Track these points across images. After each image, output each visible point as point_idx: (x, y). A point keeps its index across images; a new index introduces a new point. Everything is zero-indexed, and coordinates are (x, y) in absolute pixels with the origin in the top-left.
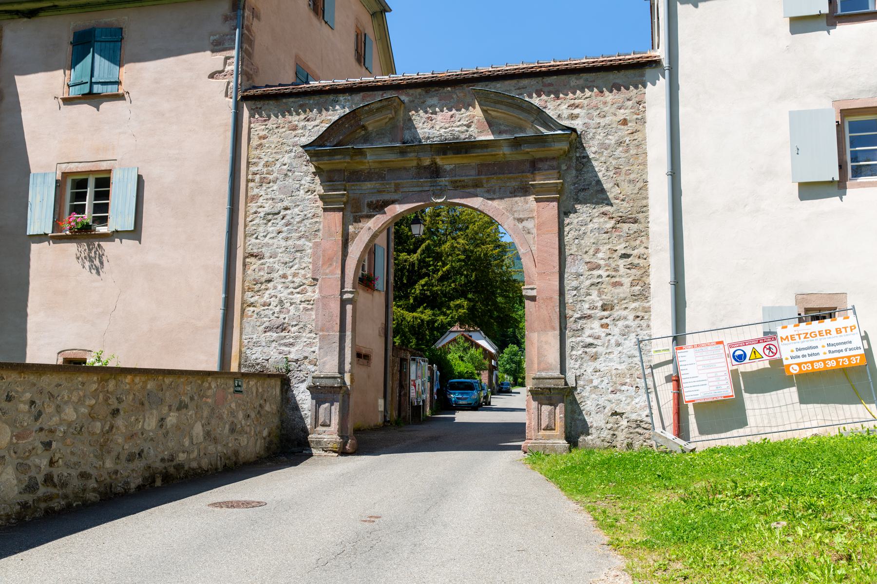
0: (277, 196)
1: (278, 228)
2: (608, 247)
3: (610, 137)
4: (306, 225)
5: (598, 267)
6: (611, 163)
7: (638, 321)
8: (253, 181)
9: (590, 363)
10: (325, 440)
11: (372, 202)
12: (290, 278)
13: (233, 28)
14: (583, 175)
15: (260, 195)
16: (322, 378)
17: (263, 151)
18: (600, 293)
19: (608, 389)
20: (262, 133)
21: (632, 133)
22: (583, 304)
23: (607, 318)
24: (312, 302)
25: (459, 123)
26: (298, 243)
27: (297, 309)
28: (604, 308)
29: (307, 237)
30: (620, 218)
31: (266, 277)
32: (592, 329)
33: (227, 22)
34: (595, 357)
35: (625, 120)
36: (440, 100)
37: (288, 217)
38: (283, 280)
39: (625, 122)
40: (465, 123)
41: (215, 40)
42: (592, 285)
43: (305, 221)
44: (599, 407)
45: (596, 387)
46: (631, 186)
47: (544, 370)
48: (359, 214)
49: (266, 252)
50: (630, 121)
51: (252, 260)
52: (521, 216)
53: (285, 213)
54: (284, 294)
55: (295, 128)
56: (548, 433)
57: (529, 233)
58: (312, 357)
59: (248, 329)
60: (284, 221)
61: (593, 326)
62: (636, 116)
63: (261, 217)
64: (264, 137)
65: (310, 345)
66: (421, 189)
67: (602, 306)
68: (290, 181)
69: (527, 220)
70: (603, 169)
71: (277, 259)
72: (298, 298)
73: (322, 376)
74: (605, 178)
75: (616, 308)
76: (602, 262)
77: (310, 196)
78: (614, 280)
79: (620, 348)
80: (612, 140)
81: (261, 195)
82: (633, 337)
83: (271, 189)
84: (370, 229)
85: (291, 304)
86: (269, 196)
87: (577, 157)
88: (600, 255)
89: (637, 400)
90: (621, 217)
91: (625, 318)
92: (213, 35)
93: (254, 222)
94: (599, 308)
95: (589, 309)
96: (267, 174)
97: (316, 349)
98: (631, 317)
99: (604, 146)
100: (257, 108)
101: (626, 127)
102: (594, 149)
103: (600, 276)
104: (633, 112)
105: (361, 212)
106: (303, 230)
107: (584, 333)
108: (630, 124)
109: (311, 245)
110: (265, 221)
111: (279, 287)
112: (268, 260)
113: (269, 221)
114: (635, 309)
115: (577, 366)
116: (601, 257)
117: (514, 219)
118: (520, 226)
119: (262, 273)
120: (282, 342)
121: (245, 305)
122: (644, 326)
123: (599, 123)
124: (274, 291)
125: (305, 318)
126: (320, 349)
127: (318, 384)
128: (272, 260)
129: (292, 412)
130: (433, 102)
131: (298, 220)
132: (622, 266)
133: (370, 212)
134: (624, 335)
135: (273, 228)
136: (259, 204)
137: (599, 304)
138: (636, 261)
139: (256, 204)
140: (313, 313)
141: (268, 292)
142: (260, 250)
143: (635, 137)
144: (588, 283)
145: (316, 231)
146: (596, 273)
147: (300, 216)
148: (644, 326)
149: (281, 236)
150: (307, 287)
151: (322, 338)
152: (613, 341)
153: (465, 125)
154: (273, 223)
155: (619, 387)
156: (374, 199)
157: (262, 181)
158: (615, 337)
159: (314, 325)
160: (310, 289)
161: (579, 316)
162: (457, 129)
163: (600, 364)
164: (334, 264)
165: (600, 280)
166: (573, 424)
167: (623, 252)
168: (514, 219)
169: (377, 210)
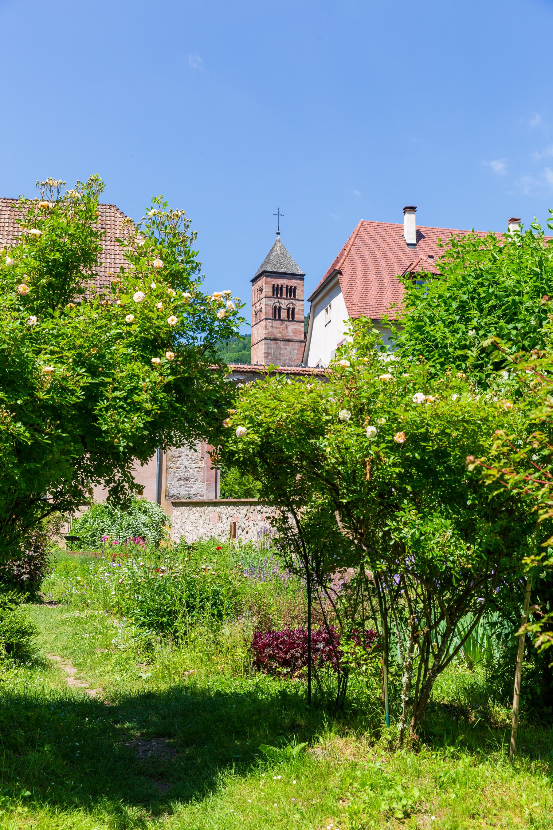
27: (194, 471)
31: (178, 455)
54: (187, 464)
58: (201, 493)
59: (169, 479)
65: (201, 488)
72: (194, 466)
111: (185, 460)
121: (168, 468)
125: (197, 475)
140: (202, 473)
151: (207, 485)
160: (200, 462)
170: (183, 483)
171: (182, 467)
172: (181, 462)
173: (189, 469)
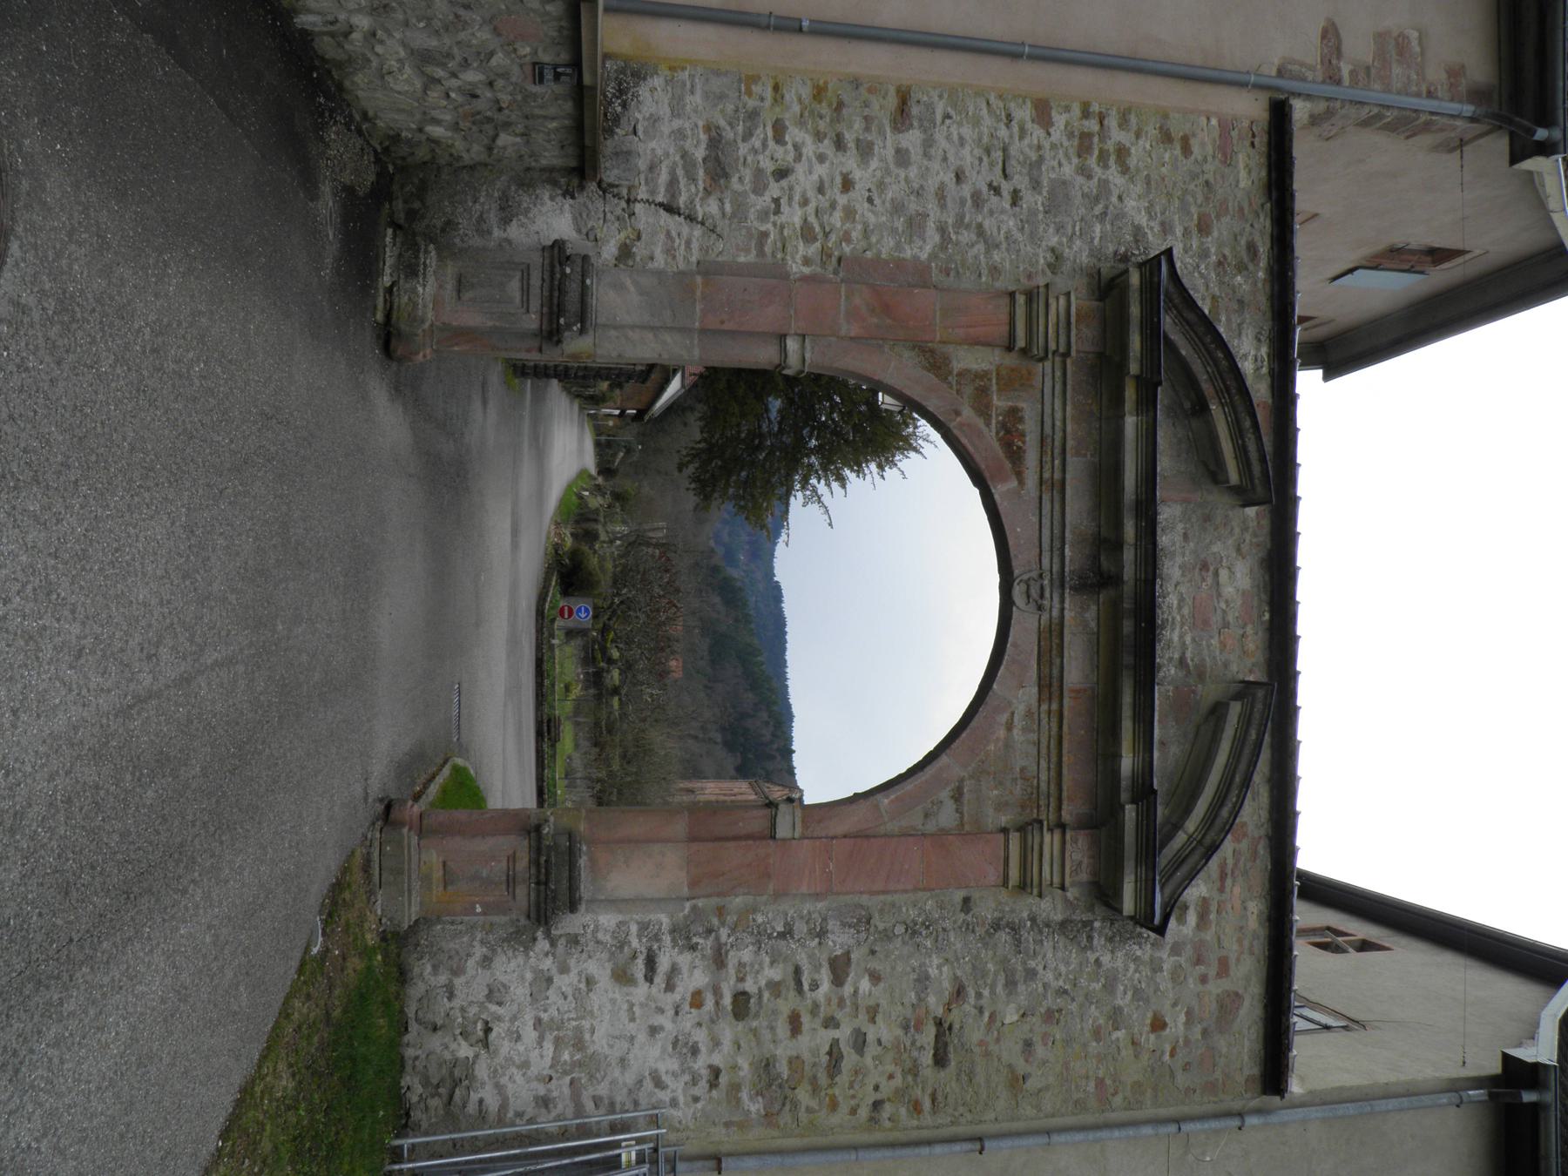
0: (1045, 173)
1: (971, 174)
2: (883, 1002)
3: (1130, 994)
4: (973, 245)
5: (838, 981)
6: (1073, 1000)
7: (705, 1072)
8: (1086, 114)
9: (609, 966)
10: (420, 289)
11: (1021, 420)
12: (842, 200)
13: (1432, 89)
14: (1051, 938)
15: (1052, 130)
16: (583, 282)
17: (1154, 143)
18: (775, 987)
19: (545, 1011)
20: (1196, 149)
21: (1133, 1043)
22: (751, 948)
23: (717, 1003)
24: (779, 256)
25: (1188, 639)
26: (931, 225)
27: (764, 215)
28: (741, 999)
29: (943, 246)
30: (946, 1025)
31: (849, 137)
32: (691, 974)
33: (1444, 76)
34: (622, 977)
35: (1164, 1026)
36: (1243, 594)
37: (995, 199)
38: (838, 180)
39: (1158, 1025)
40: (1188, 655)
41: (1409, 42)
42: (798, 971)
43: (980, 247)
44: (502, 989)
45: (550, 980)
46: (1019, 1047)
47: (592, 860)
48: (994, 388)
49: (912, 139)
50: (1158, 1037)
51: (892, 101)
52: (967, 796)
53: (1005, 193)
54: (804, 179)
55: (1204, 228)
56: (438, 874)
57: (926, 816)
60: (985, 189)
61: (698, 973)
62: (1168, 1048)
63: (996, 129)
64: (1186, 150)
65: (670, 251)
66: (1046, 546)
67: (744, 993)
68: (1082, 211)
69: (957, 811)
70: (1061, 983)
71: (892, 166)
73: (588, 282)
74: (1041, 989)
75: (741, 1026)
76: (848, 989)
77: (1042, 261)
78: (806, 1019)
79: (642, 1037)
80: (1123, 1000)
81: (1049, 134)
82: (674, 1065)
83: (1064, 161)
84: (958, 413)
85: (777, 201)
86: (1048, 154)
87: (1092, 922)
88: (865, 985)
89: (518, 1078)
90: (950, 1028)
91: (716, 1043)
92: (1420, 39)
93: (985, 111)
94: (740, 987)
95: (740, 963)
96: (1101, 151)
97: (660, 261)
98: (717, 1060)
99: (1109, 987)
100: (1254, 136)
101: (1147, 1028)
102: (1106, 959)
103: (815, 986)
104: (1178, 1042)
105: (999, 390)
106: (960, 237)
107: (681, 953)
108: (1152, 1037)
109: (924, 256)
110: (985, 139)
111: (821, 170)
112: (889, 143)
113: (988, 152)
114: (735, 1068)
115: (600, 936)
116: (861, 991)
117: (962, 780)
118: (945, 794)
119: (858, 125)
120: (680, 172)
122: (697, 1091)
123: (1161, 969)
124: (811, 154)
126: (659, 274)
127: (568, 270)
128: (890, 153)
129: (496, 195)
130: (1238, 575)
131: (986, 224)
132: (836, 1034)
133: (997, 415)
134: (675, 1043)
135: (969, 159)
136: (1029, 125)
137: (749, 986)
138: (847, 1065)
139: (1028, 118)
141: (809, 140)
142: (915, 124)
143: (1124, 1053)
144: (802, 959)
145: (958, 272)
146: (825, 976)
147: (995, 230)
148: (697, 1091)
149: (949, 178)
150: (818, 244)
152: (659, 1020)
153: (1184, 653)
154: (981, 160)
155: (549, 1037)
156: (1030, 427)
157: (1084, 143)
158: (668, 1025)
159: (720, 259)
161: (724, 938)
162: (1176, 638)
163: (606, 992)
164: (875, 320)
165: (806, 987)
166: (460, 927)
167: (871, 1037)
168: (962, 780)
169: (1002, 433)
170: (700, 154)
171: (784, 154)
172: (809, 149)
173: (774, 189)
